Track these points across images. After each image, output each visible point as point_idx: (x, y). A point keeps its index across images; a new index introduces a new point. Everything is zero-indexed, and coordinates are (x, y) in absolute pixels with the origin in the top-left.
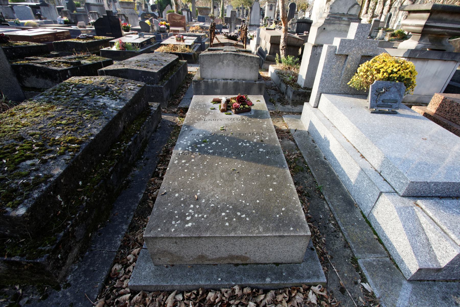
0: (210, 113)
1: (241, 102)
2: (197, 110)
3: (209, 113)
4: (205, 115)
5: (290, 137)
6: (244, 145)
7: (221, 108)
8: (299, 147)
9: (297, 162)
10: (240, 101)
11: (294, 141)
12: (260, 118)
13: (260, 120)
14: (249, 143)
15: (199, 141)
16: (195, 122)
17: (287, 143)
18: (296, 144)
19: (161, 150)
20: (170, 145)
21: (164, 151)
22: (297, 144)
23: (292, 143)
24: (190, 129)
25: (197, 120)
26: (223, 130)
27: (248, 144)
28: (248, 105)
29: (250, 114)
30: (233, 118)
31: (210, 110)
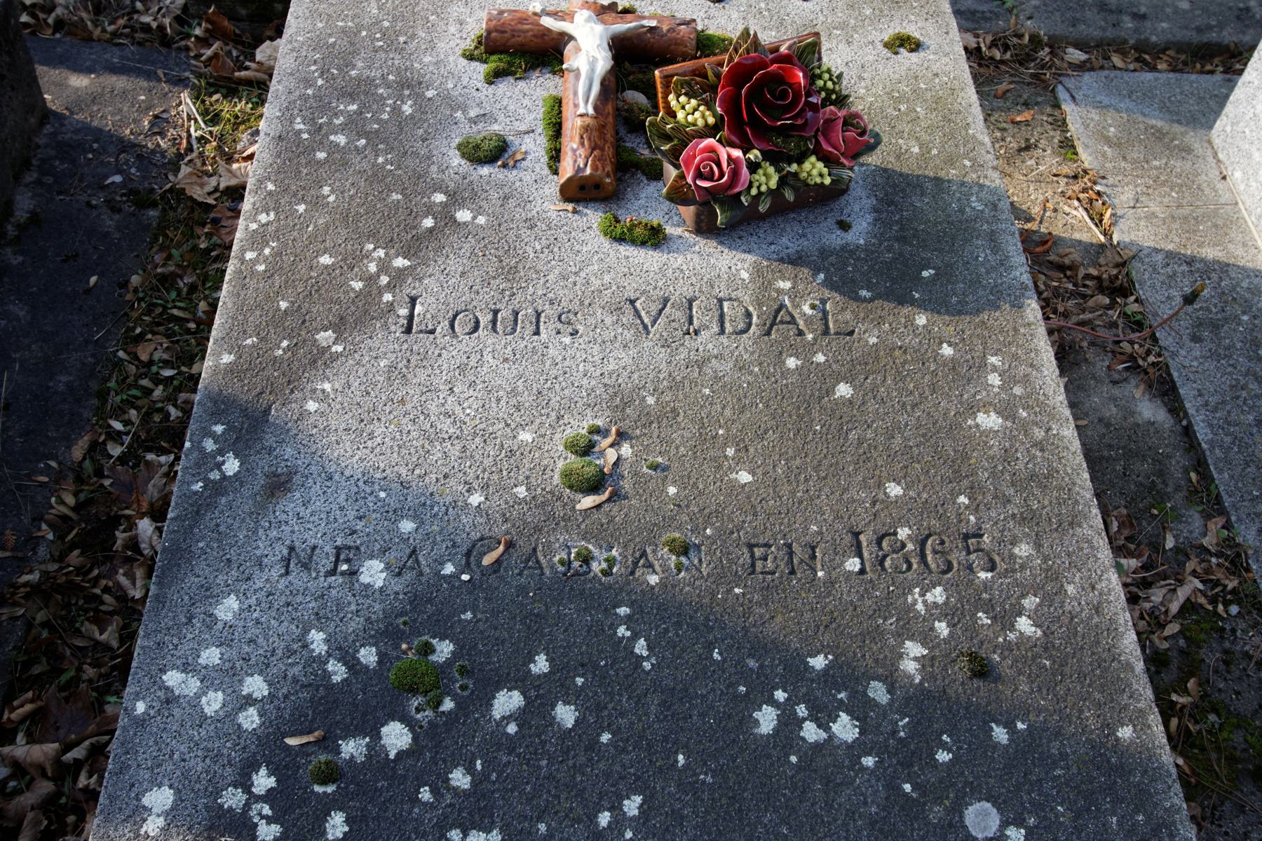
0: (463, 215)
1: (763, 132)
2: (340, 159)
3: (446, 217)
4: (415, 245)
5: (1132, 344)
6: (811, 732)
7: (567, 168)
8: (1222, 479)
9: (1211, 658)
10: (755, 122)
11: (1166, 390)
12: (936, 305)
13: (944, 325)
14: (861, 709)
15: (353, 664)
16: (320, 359)
17: (1111, 411)
18: (1188, 431)
19: (37, 519)
20: (116, 437)
21: (62, 525)
22: (1203, 433)
23: (1150, 410)
24: (263, 464)
25: (340, 327)
26: (594, 485)
27: (845, 728)
28: (827, 159)
29: (836, 239)
30: (682, 290)
31: (456, 160)
